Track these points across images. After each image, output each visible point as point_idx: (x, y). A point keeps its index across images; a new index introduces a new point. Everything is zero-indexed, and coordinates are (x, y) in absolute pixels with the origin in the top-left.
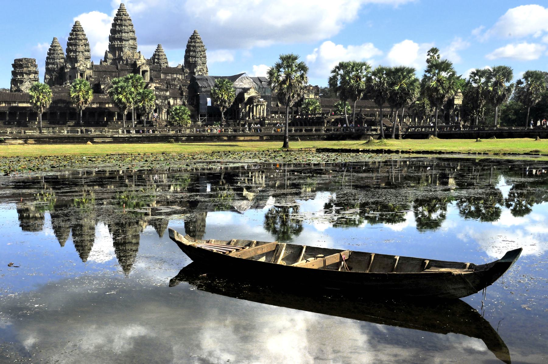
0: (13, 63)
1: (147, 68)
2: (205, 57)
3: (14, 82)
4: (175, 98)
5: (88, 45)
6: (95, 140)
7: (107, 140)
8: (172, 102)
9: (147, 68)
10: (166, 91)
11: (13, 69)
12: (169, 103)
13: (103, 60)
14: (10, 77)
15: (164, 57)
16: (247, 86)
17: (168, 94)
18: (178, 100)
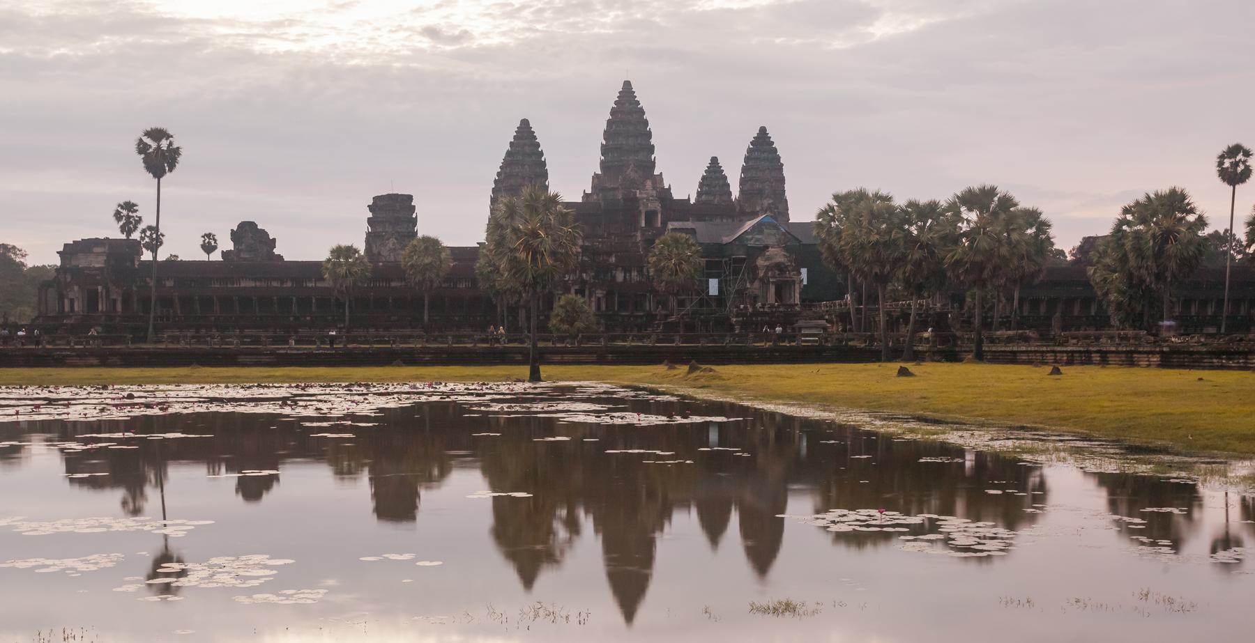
0: (371, 203)
1: (657, 206)
2: (782, 180)
3: (370, 238)
4: (627, 270)
5: (544, 164)
6: (241, 359)
7: (265, 359)
8: (620, 277)
9: (657, 206)
10: (610, 254)
11: (370, 215)
12: (614, 277)
13: (589, 191)
14: (365, 228)
15: (721, 182)
16: (770, 242)
17: (613, 260)
18: (634, 274)
